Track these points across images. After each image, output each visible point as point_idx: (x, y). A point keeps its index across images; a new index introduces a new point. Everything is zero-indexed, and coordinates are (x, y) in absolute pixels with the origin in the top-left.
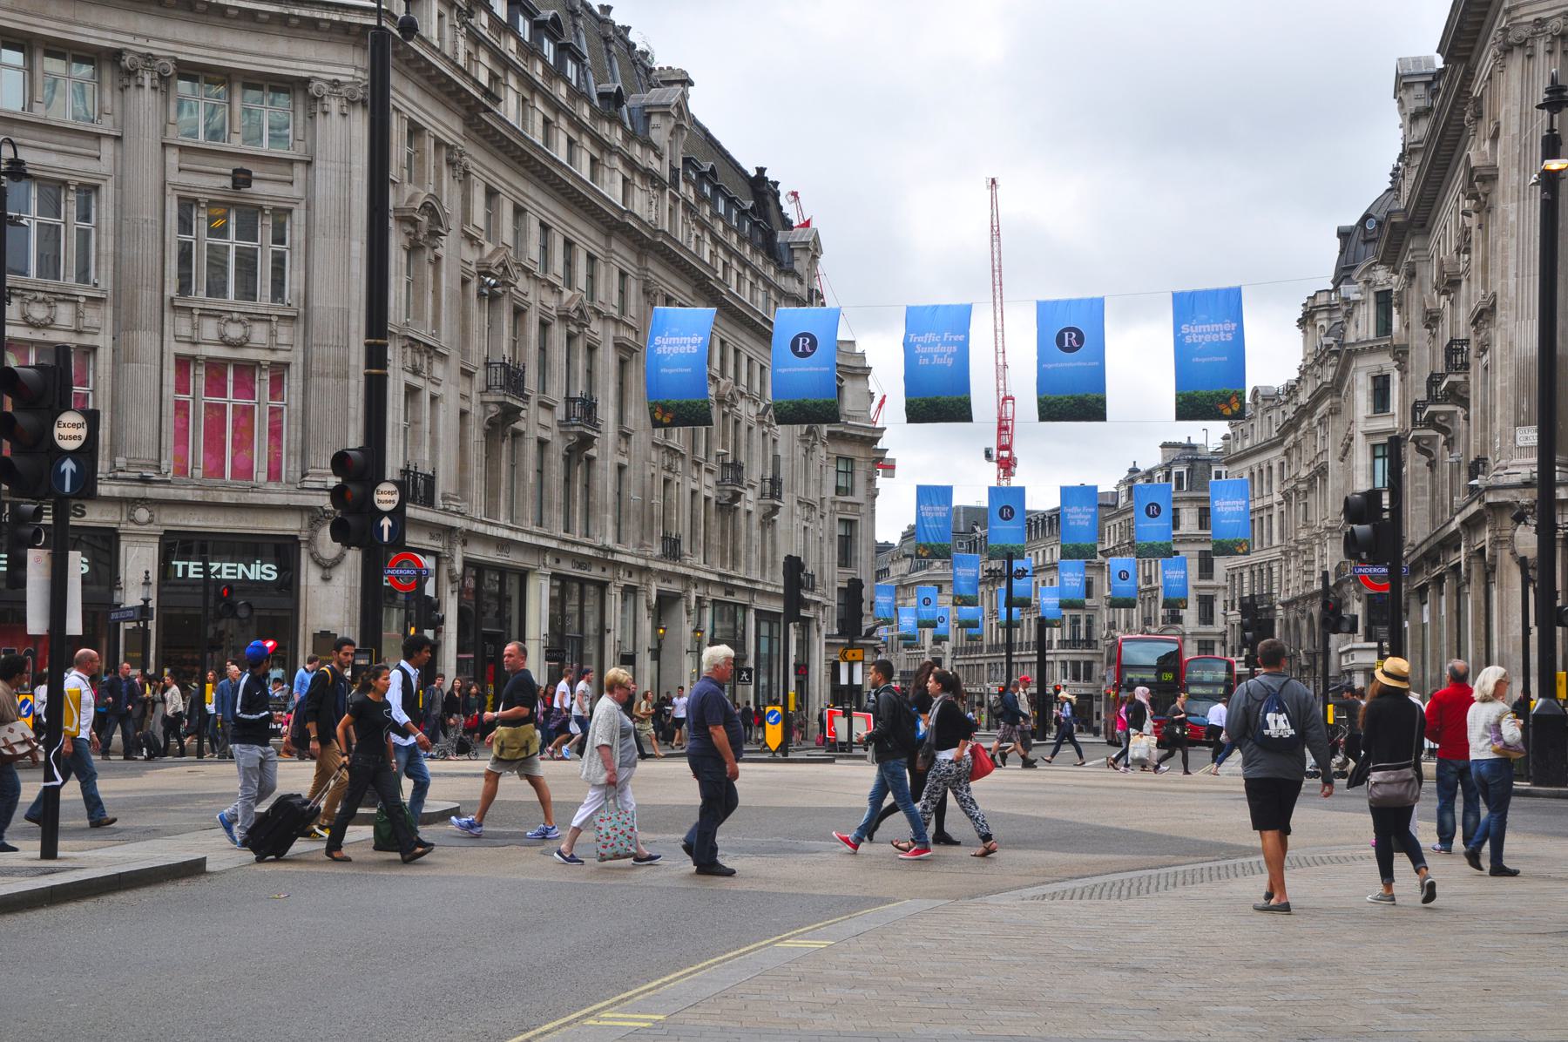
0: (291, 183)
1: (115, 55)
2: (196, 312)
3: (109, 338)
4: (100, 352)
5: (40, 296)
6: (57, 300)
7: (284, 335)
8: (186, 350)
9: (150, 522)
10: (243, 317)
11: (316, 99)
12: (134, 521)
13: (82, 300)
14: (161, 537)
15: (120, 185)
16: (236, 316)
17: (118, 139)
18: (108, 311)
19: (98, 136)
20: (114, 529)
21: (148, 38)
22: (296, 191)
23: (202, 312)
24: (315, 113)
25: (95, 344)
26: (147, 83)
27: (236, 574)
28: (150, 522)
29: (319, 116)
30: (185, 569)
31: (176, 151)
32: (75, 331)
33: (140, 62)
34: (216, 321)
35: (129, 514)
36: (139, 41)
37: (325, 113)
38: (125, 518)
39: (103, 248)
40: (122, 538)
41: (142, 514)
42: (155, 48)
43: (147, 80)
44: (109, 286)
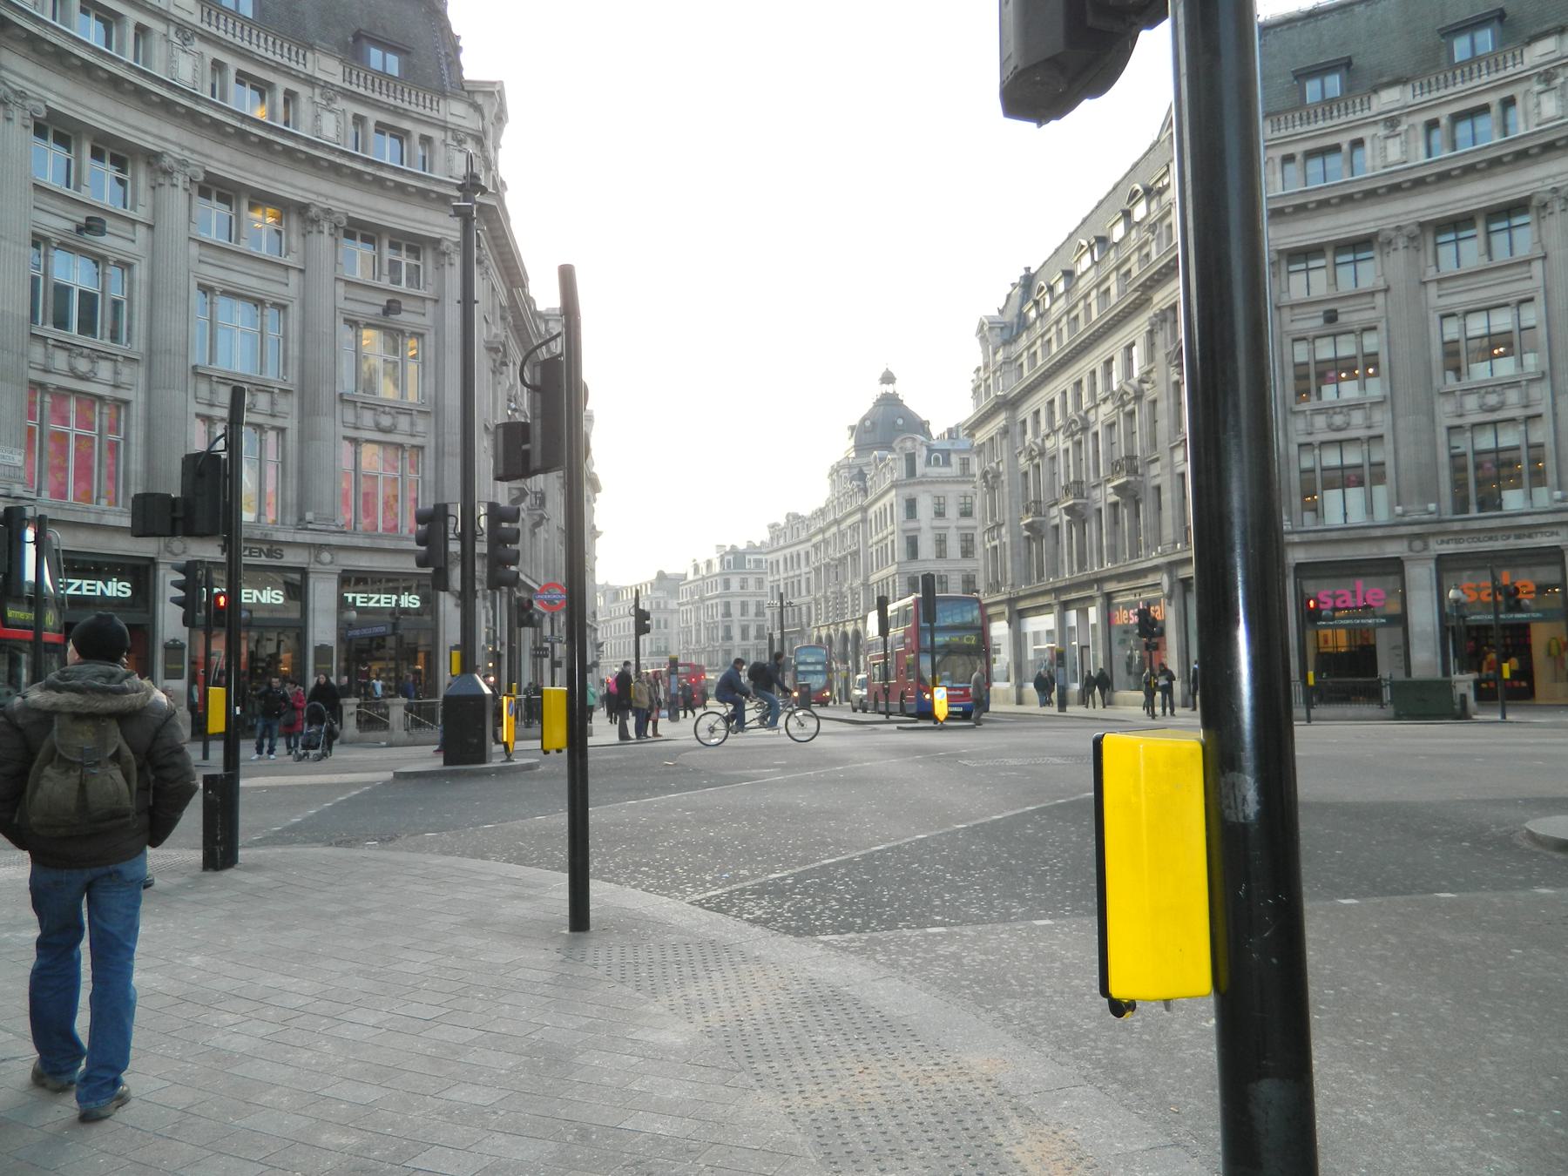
0: (424, 315)
1: (302, 209)
2: (359, 405)
3: (295, 422)
4: (289, 432)
7: (421, 424)
9: (331, 563)
10: (393, 411)
11: (444, 254)
12: (320, 563)
13: (276, 391)
14: (339, 575)
15: (303, 307)
16: (387, 409)
17: (302, 271)
18: (294, 400)
19: (287, 268)
21: (327, 197)
22: (427, 321)
24: (443, 265)
25: (285, 425)
26: (326, 231)
29: (447, 266)
30: (354, 599)
31: (342, 284)
32: (271, 415)
33: (322, 215)
34: (372, 412)
35: (316, 557)
36: (320, 199)
38: (312, 560)
39: (290, 352)
40: (311, 575)
41: (326, 557)
42: (331, 204)
43: (326, 227)
44: (296, 381)
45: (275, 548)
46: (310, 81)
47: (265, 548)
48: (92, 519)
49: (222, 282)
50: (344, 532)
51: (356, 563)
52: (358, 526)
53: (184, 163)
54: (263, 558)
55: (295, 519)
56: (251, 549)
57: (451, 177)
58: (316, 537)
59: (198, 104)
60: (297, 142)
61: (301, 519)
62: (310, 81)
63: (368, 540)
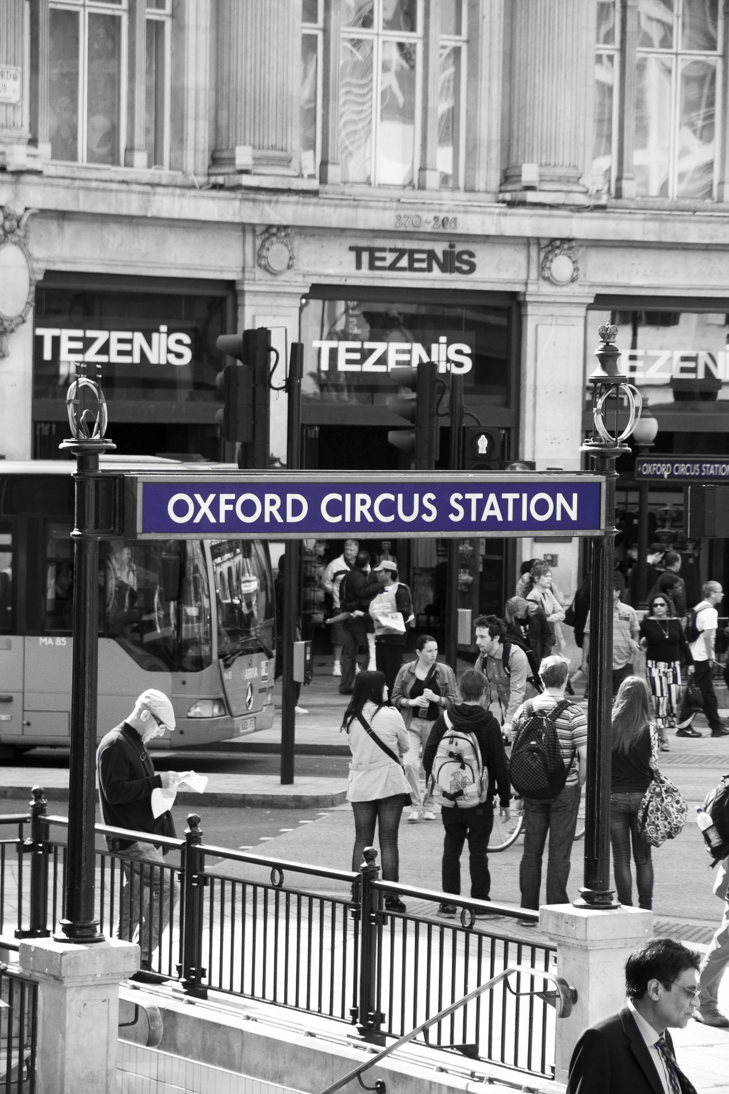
12: (547, 279)
20: (514, 295)
27: (694, 370)
28: (573, 280)
35: (542, 267)
38: (534, 274)
40: (530, 309)
45: (459, 248)
47: (440, 248)
48: (132, 205)
50: (603, 208)
51: (624, 280)
52: (625, 184)
54: (436, 271)
55: (495, 177)
56: (412, 252)
58: (545, 222)
61: (508, 176)
63: (653, 226)
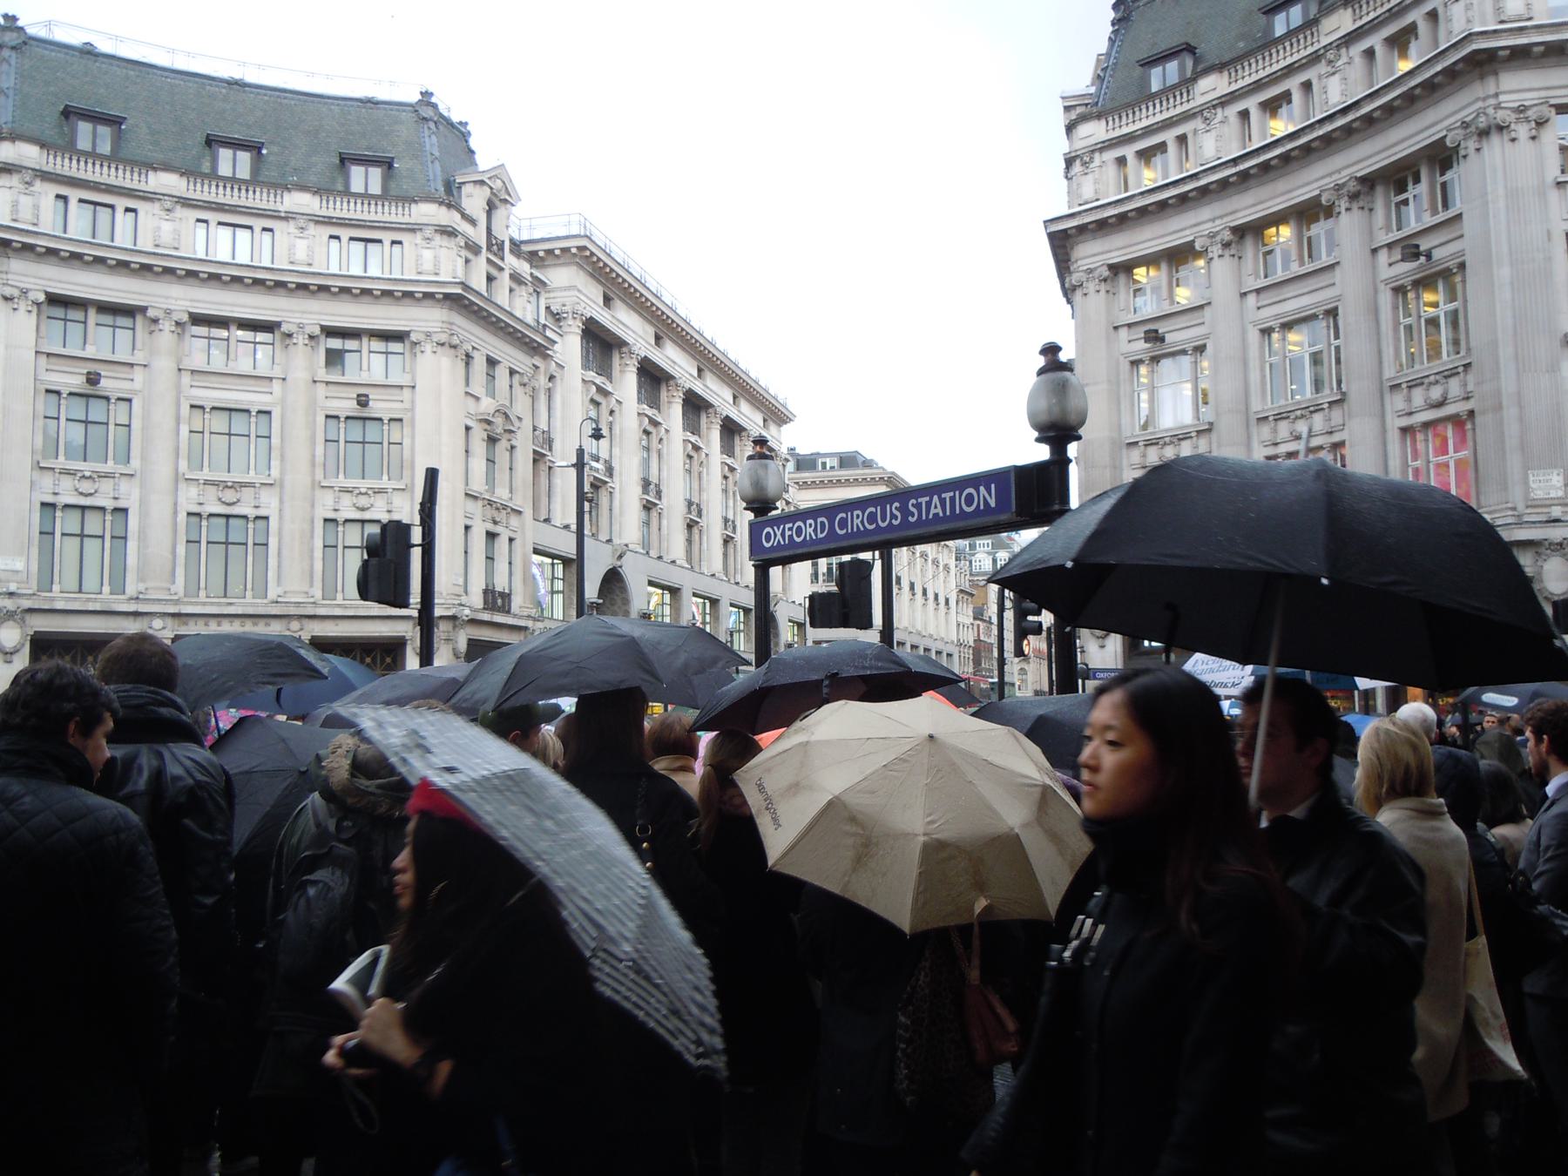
5: (1299, 413)
6: (1311, 412)
8: (1405, 422)
16: (1432, 378)
23: (1410, 384)
25: (1343, 438)
37: (1465, 157)
42: (1342, 177)
46: (1315, 59)
49: (1277, 316)
53: (1212, 236)
57: (1502, 22)
59: (1198, 179)
60: (1283, 145)
62: (1315, 59)
